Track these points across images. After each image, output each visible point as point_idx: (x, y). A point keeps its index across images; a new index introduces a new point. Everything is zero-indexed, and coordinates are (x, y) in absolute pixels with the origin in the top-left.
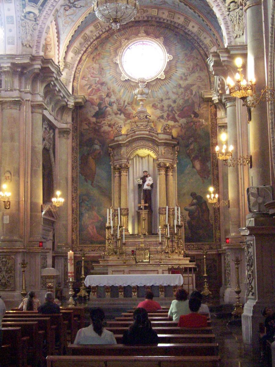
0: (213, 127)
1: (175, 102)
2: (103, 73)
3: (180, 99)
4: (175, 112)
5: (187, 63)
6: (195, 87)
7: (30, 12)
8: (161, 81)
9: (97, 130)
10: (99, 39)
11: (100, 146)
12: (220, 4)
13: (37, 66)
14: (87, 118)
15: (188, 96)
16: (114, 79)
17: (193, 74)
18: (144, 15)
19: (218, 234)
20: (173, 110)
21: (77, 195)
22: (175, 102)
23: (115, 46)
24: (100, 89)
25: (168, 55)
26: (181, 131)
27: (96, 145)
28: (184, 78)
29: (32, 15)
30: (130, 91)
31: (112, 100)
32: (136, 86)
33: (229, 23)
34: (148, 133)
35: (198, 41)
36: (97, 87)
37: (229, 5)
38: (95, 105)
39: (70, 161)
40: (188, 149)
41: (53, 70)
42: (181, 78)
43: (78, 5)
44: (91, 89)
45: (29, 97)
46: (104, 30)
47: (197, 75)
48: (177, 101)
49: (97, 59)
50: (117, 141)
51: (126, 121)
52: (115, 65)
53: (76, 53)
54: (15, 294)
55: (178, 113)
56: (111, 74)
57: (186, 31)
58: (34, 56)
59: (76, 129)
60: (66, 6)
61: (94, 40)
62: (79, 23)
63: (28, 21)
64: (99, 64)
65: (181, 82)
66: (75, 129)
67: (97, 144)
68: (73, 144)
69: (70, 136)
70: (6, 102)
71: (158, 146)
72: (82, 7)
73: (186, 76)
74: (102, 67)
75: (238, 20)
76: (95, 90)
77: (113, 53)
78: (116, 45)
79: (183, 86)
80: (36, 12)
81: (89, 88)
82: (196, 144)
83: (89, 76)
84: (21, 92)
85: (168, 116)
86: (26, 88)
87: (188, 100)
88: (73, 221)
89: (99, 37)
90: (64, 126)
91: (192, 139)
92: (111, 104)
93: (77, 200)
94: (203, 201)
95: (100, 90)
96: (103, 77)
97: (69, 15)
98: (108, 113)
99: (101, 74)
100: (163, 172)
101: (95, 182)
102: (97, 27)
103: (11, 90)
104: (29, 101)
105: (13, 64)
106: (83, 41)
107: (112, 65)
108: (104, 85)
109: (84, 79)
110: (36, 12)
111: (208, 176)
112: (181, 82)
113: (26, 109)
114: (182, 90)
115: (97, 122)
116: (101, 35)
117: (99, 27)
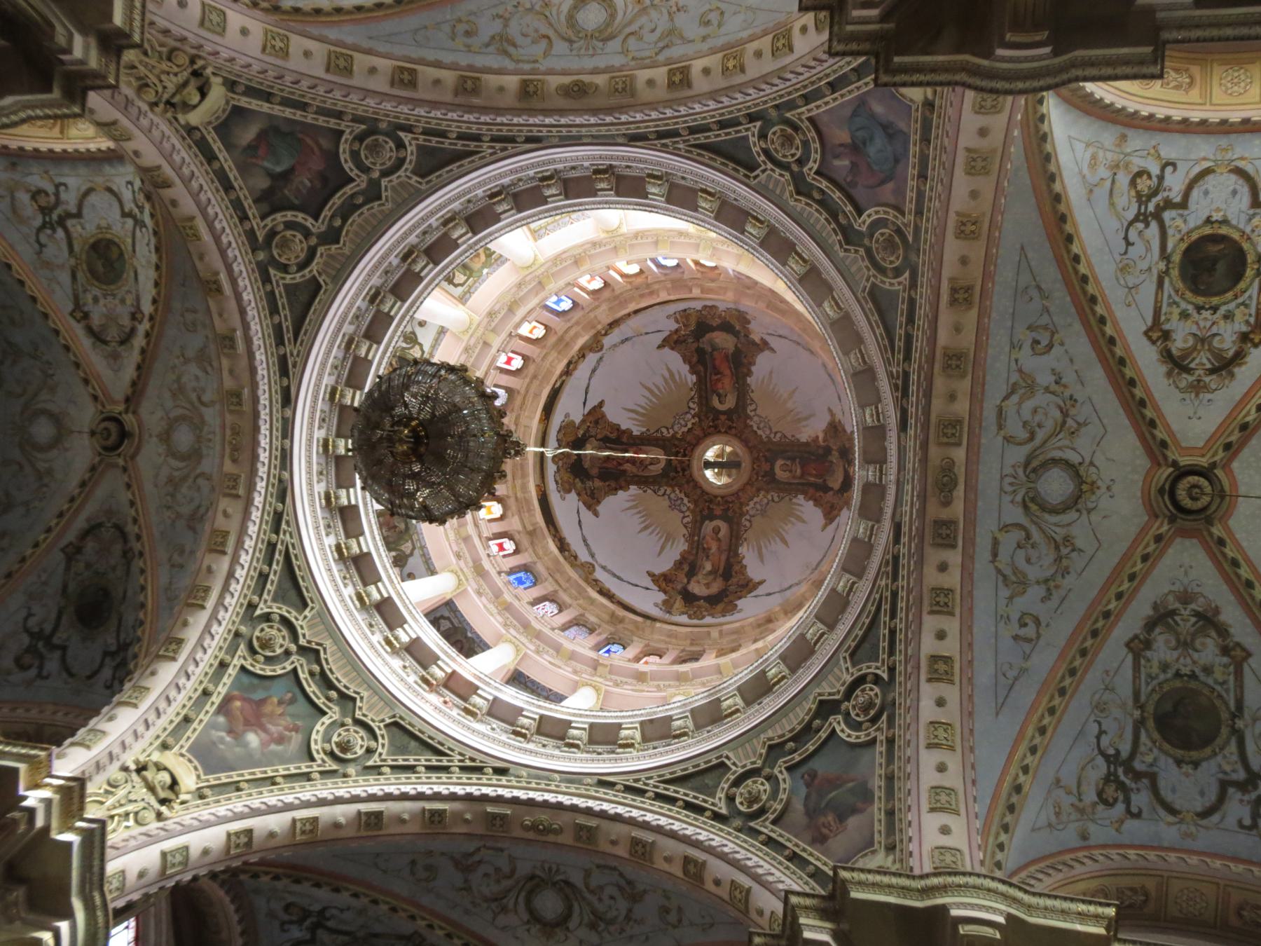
12: (153, 732)
29: (196, 98)
43: (50, 237)
60: (52, 199)
63: (181, 79)
72: (37, 246)
75: (121, 811)
80: (194, 118)
97: (13, 198)
110: (194, 118)
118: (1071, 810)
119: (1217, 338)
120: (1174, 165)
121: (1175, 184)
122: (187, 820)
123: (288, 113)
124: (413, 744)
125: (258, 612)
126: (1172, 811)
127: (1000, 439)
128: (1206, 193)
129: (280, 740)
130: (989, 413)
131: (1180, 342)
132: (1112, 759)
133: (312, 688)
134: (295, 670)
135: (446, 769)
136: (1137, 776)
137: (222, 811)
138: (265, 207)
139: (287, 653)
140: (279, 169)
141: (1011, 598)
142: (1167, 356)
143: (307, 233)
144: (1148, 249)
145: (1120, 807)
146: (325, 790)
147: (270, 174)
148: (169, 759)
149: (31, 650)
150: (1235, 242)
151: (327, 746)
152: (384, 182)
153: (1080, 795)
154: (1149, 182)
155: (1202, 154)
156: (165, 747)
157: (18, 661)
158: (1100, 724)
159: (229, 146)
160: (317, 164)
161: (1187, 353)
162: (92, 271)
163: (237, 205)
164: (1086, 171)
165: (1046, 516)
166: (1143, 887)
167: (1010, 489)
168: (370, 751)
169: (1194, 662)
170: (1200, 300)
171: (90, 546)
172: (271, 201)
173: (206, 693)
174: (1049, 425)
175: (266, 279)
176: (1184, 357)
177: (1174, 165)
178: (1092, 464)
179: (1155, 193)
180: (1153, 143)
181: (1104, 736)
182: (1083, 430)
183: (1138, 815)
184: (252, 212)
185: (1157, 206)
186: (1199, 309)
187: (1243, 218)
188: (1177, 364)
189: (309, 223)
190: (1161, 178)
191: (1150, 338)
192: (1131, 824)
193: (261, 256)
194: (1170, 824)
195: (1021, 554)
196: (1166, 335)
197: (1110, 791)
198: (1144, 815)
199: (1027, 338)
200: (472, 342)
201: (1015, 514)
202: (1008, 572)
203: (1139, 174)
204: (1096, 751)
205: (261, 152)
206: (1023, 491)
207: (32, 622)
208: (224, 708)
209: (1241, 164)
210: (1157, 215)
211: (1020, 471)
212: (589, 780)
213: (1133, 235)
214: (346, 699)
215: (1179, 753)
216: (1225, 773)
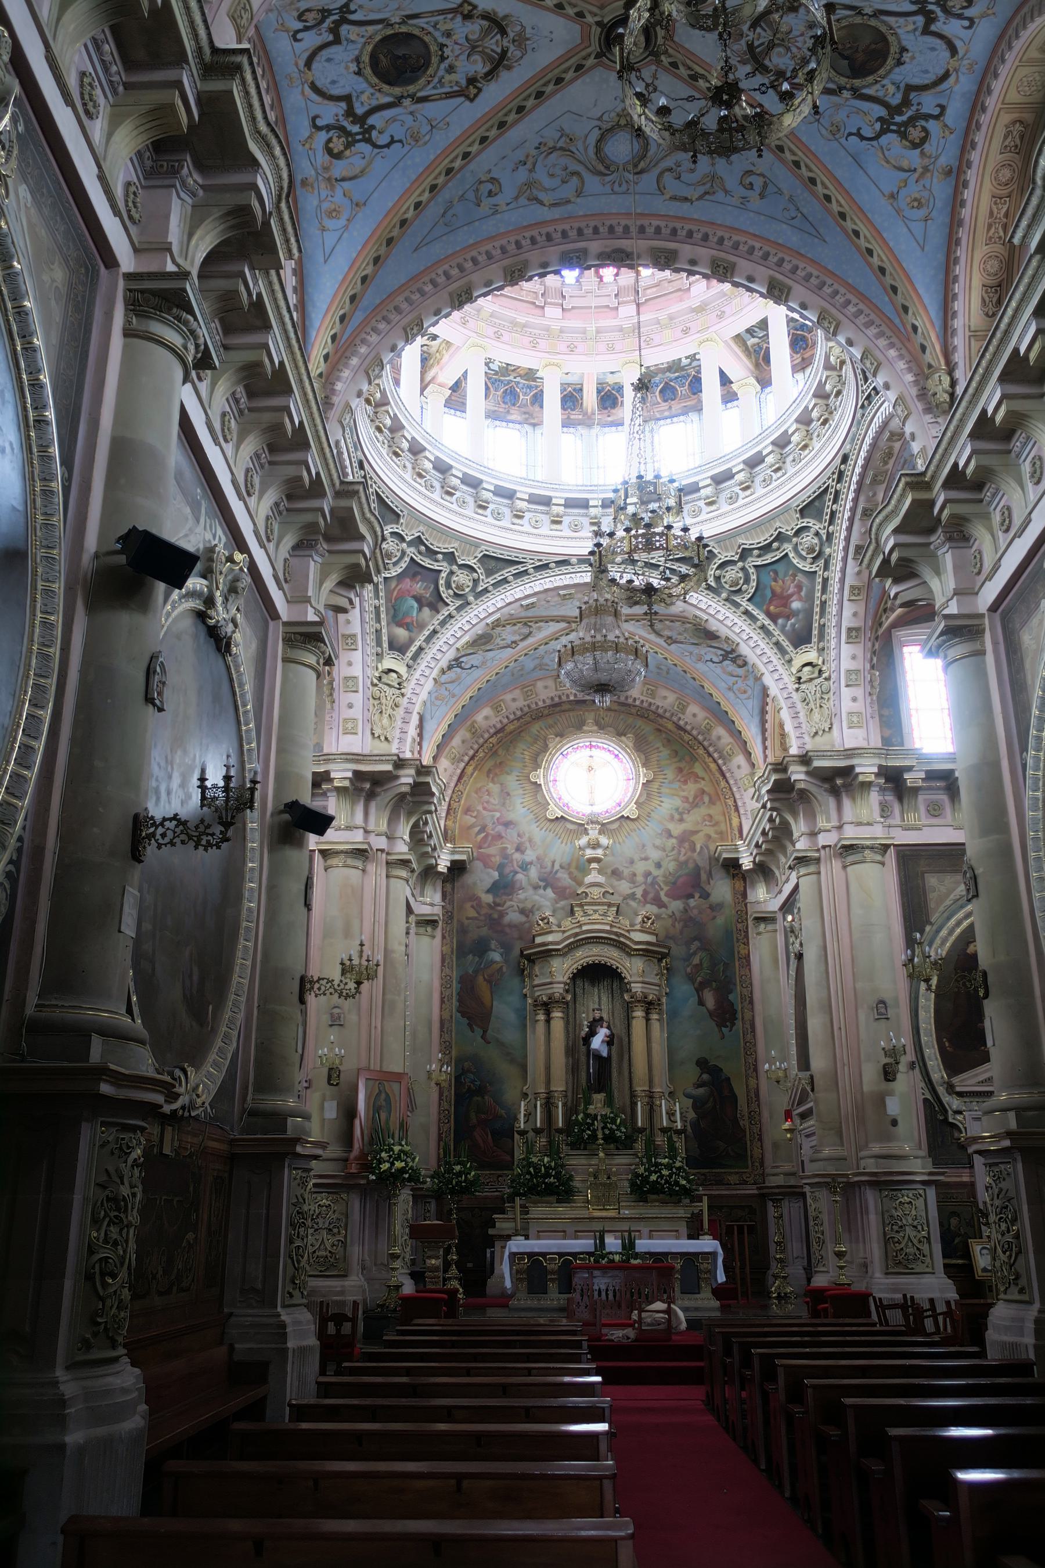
1: (658, 865)
6: (701, 834)
7: (390, 671)
9: (494, 921)
12: (779, 667)
13: (407, 777)
16: (531, 816)
19: (757, 1152)
20: (654, 883)
22: (658, 865)
25: (642, 771)
28: (677, 816)
31: (528, 859)
32: (582, 829)
33: (800, 706)
34: (608, 928)
35: (706, 743)
37: (800, 671)
39: (437, 984)
41: (434, 789)
42: (672, 818)
45: (381, 843)
46: (512, 717)
47: (703, 811)
48: (664, 864)
50: (544, 944)
53: (455, 760)
54: (346, 1283)
55: (666, 888)
57: (681, 723)
58: (400, 760)
59: (451, 918)
62: (465, 700)
63: (386, 688)
65: (671, 826)
66: (449, 915)
69: (438, 933)
70: (338, 853)
71: (629, 955)
73: (681, 814)
80: (402, 670)
83: (480, 808)
84: (366, 832)
85: (645, 893)
86: (377, 824)
87: (686, 862)
89: (502, 730)
90: (426, 910)
91: (697, 944)
92: (525, 867)
98: (518, 885)
100: (639, 1013)
103: (348, 828)
104: (382, 851)
105: (356, 773)
106: (468, 735)
107: (528, 787)
110: (402, 670)
113: (376, 871)
118: (921, 182)
119: (471, 37)
120: (314, 119)
121: (331, 112)
122: (833, 666)
123: (383, 616)
124: (817, 504)
125: (713, 584)
126: (946, 76)
127: (579, 200)
128: (333, 82)
129: (799, 587)
130: (557, 213)
131: (479, 67)
132: (886, 126)
133: (769, 558)
134: (755, 566)
135: (837, 493)
136: (906, 102)
137: (833, 644)
138: (441, 604)
139: (743, 569)
140: (416, 605)
141: (726, 192)
142: (490, 75)
143: (452, 573)
144: (393, 120)
145: (932, 125)
146: (835, 575)
147: (420, 609)
148: (798, 662)
149: (734, 661)
150: (376, 46)
151: (809, 560)
152: (408, 539)
153: (909, 171)
154: (335, 139)
155: (300, 97)
156: (790, 661)
157: (740, 667)
158: (850, 134)
159: (411, 641)
160: (407, 583)
161: (487, 57)
162: (485, 644)
163: (443, 623)
164: (342, 222)
165: (650, 153)
166: (1007, 127)
167: (624, 185)
168: (817, 534)
169: (802, 35)
170: (435, 60)
171: (667, 633)
172: (436, 602)
173: (763, 627)
174: (565, 161)
175: (486, 591)
176: (491, 59)
177: (314, 119)
178: (600, 119)
179: (342, 129)
180: (300, 148)
181: (862, 132)
182: (567, 131)
183: (943, 108)
184: (445, 612)
185: (353, 122)
186: (443, 58)
187: (351, 46)
188: (499, 63)
189: (444, 575)
190: (328, 128)
191: (476, 96)
192: (949, 118)
193: (471, 598)
194: (957, 80)
195: (685, 177)
196: (472, 81)
197: (915, 134)
198: (944, 102)
199: (487, 202)
200: (490, 331)
201: (649, 180)
202: (701, 190)
203: (329, 151)
204: (874, 143)
205: (408, 620)
206: (626, 174)
207: (715, 659)
208: (773, 618)
209: (301, 63)
210: (361, 120)
211: (608, 179)
212: (858, 415)
213: (383, 140)
214: (780, 538)
215: (890, 62)
216: (915, 30)
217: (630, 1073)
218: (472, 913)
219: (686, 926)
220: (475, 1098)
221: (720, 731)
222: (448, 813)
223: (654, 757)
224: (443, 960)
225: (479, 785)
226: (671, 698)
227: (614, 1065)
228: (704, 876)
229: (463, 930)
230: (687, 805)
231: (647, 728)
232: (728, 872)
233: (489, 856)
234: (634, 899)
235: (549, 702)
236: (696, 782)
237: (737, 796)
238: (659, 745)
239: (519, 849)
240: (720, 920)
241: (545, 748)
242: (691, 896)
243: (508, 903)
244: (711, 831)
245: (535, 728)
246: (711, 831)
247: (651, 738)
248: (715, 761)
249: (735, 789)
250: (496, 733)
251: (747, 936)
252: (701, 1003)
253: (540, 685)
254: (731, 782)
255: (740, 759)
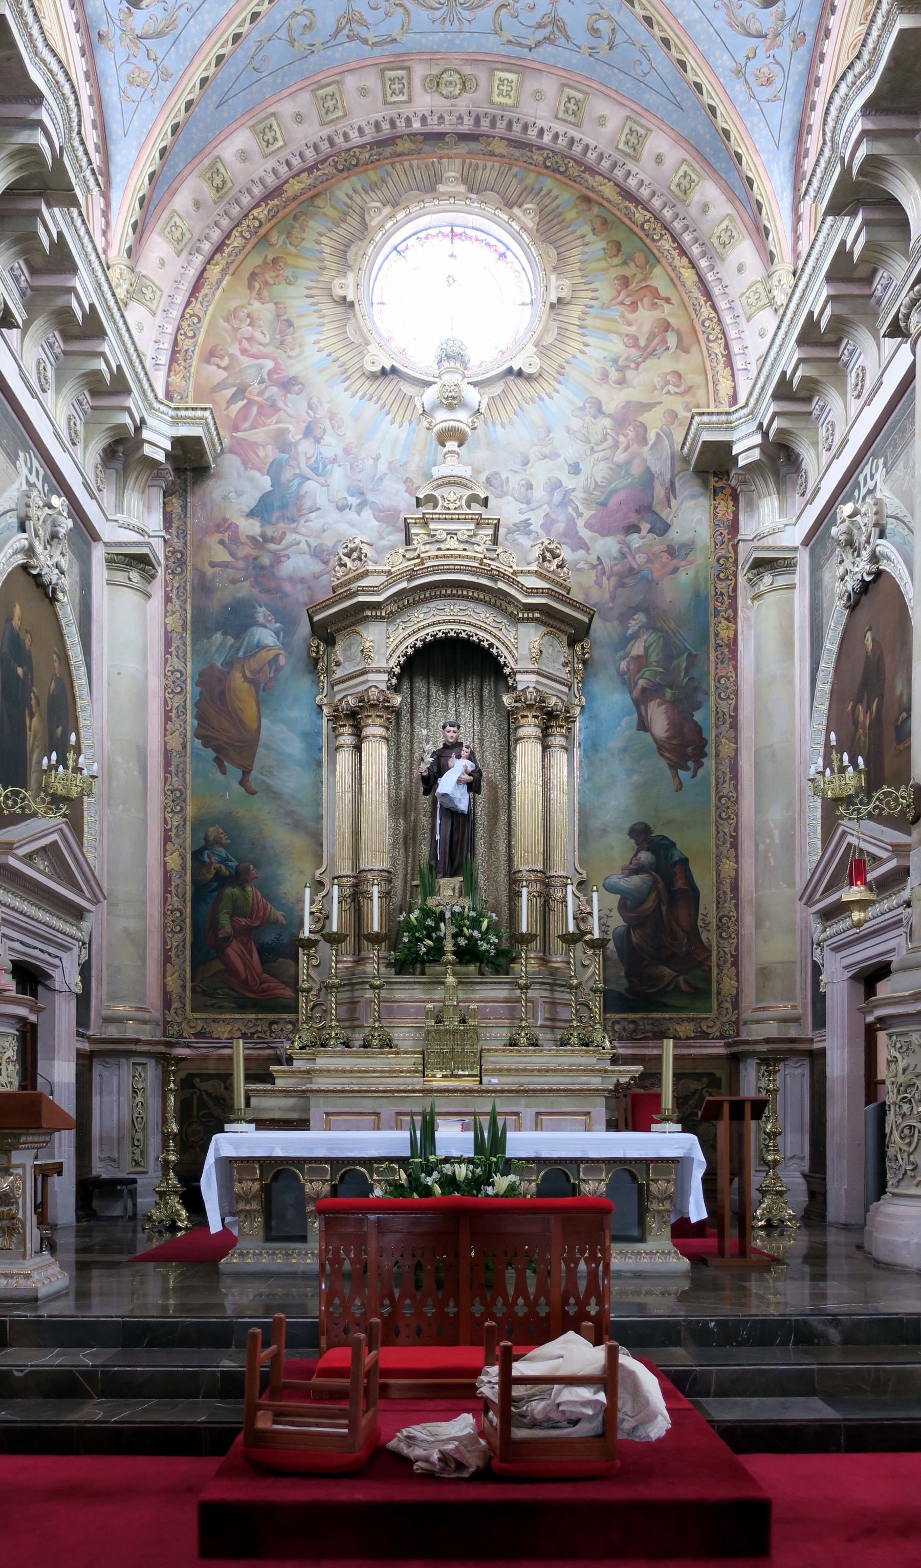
0: (722, 575)
1: (575, 469)
2: (289, 338)
3: (599, 461)
4: (576, 509)
5: (631, 317)
6: (658, 411)
8: (521, 383)
10: (276, 202)
11: (277, 633)
14: (225, 520)
15: (627, 448)
16: (335, 368)
17: (649, 361)
18: (464, 103)
21: (185, 820)
22: (575, 469)
23: (342, 232)
24: (281, 404)
26: (599, 584)
27: (261, 629)
28: (614, 375)
30: (398, 419)
31: (328, 453)
35: (677, 226)
36: (266, 395)
38: (259, 470)
40: (623, 659)
42: (605, 376)
44: (241, 404)
49: (266, 283)
51: (381, 538)
52: (339, 309)
53: (179, 244)
55: (588, 514)
56: (322, 344)
57: (632, 182)
59: (181, 563)
61: (257, 205)
64: (276, 304)
65: (602, 393)
66: (178, 560)
67: (264, 626)
68: (169, 620)
73: (621, 369)
74: (284, 318)
76: (261, 407)
77: (330, 261)
78: (343, 231)
79: (610, 407)
81: (233, 399)
82: (653, 637)
83: (234, 350)
87: (628, 463)
88: (169, 921)
89: (277, 191)
91: (640, 618)
93: (184, 841)
94: (676, 858)
95: (279, 410)
96: (290, 357)
98: (307, 504)
99: (282, 343)
101: (254, 773)
102: (269, 136)
107: (330, 309)
108: (296, 388)
109: (213, 359)
111: (699, 765)
112: (602, 393)
114: (607, 422)
115: (263, 535)
116: (287, 182)
117: (275, 139)
217: (509, 846)
218: (221, 555)
219: (621, 585)
220: (229, 891)
221: (708, 191)
222: (173, 359)
223: (575, 255)
224: (168, 643)
225: (233, 304)
226: (615, 117)
227: (480, 832)
228: (659, 492)
229: (203, 588)
230: (634, 352)
231: (565, 196)
232: (705, 484)
233: (253, 445)
234: (529, 533)
235: (370, 135)
236: (654, 305)
237: (732, 333)
238: (586, 229)
239: (308, 432)
240: (685, 576)
241: (363, 231)
242: (633, 529)
243: (290, 538)
244: (677, 404)
245: (343, 189)
246: (677, 404)
247: (571, 215)
248: (693, 265)
249: (728, 319)
250: (266, 198)
251: (734, 606)
252: (643, 725)
253: (351, 83)
254: (722, 304)
255: (744, 251)
